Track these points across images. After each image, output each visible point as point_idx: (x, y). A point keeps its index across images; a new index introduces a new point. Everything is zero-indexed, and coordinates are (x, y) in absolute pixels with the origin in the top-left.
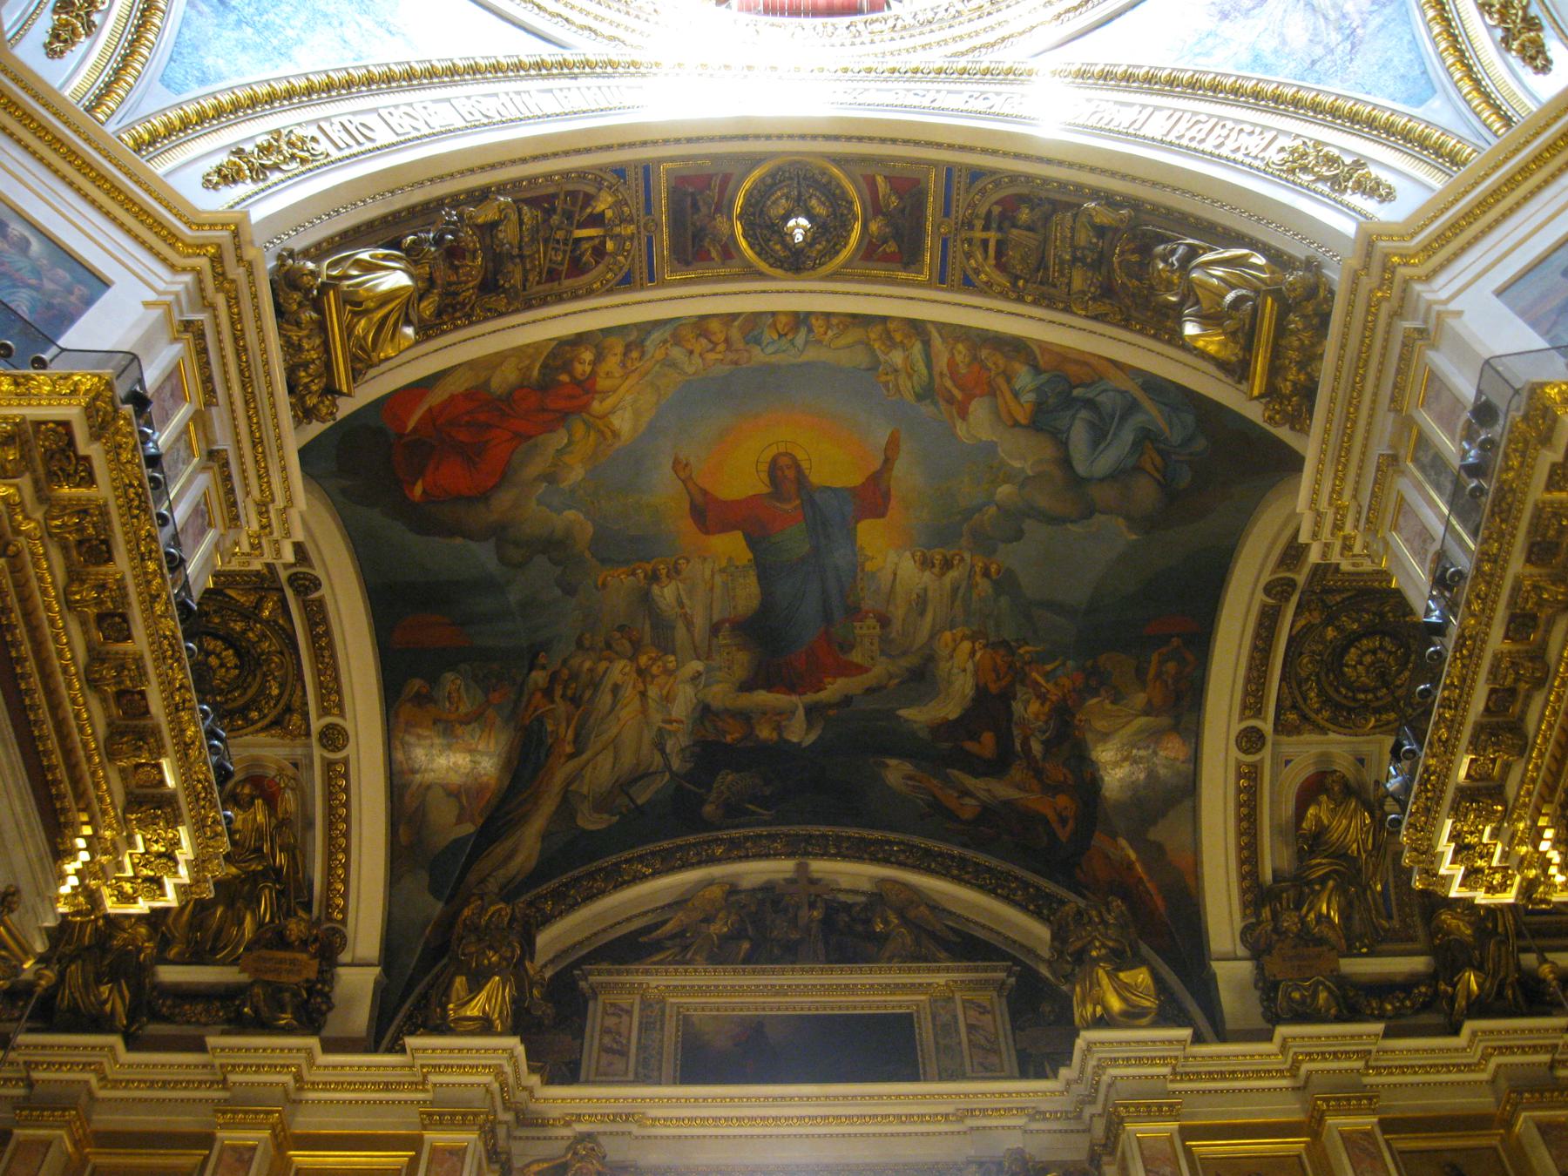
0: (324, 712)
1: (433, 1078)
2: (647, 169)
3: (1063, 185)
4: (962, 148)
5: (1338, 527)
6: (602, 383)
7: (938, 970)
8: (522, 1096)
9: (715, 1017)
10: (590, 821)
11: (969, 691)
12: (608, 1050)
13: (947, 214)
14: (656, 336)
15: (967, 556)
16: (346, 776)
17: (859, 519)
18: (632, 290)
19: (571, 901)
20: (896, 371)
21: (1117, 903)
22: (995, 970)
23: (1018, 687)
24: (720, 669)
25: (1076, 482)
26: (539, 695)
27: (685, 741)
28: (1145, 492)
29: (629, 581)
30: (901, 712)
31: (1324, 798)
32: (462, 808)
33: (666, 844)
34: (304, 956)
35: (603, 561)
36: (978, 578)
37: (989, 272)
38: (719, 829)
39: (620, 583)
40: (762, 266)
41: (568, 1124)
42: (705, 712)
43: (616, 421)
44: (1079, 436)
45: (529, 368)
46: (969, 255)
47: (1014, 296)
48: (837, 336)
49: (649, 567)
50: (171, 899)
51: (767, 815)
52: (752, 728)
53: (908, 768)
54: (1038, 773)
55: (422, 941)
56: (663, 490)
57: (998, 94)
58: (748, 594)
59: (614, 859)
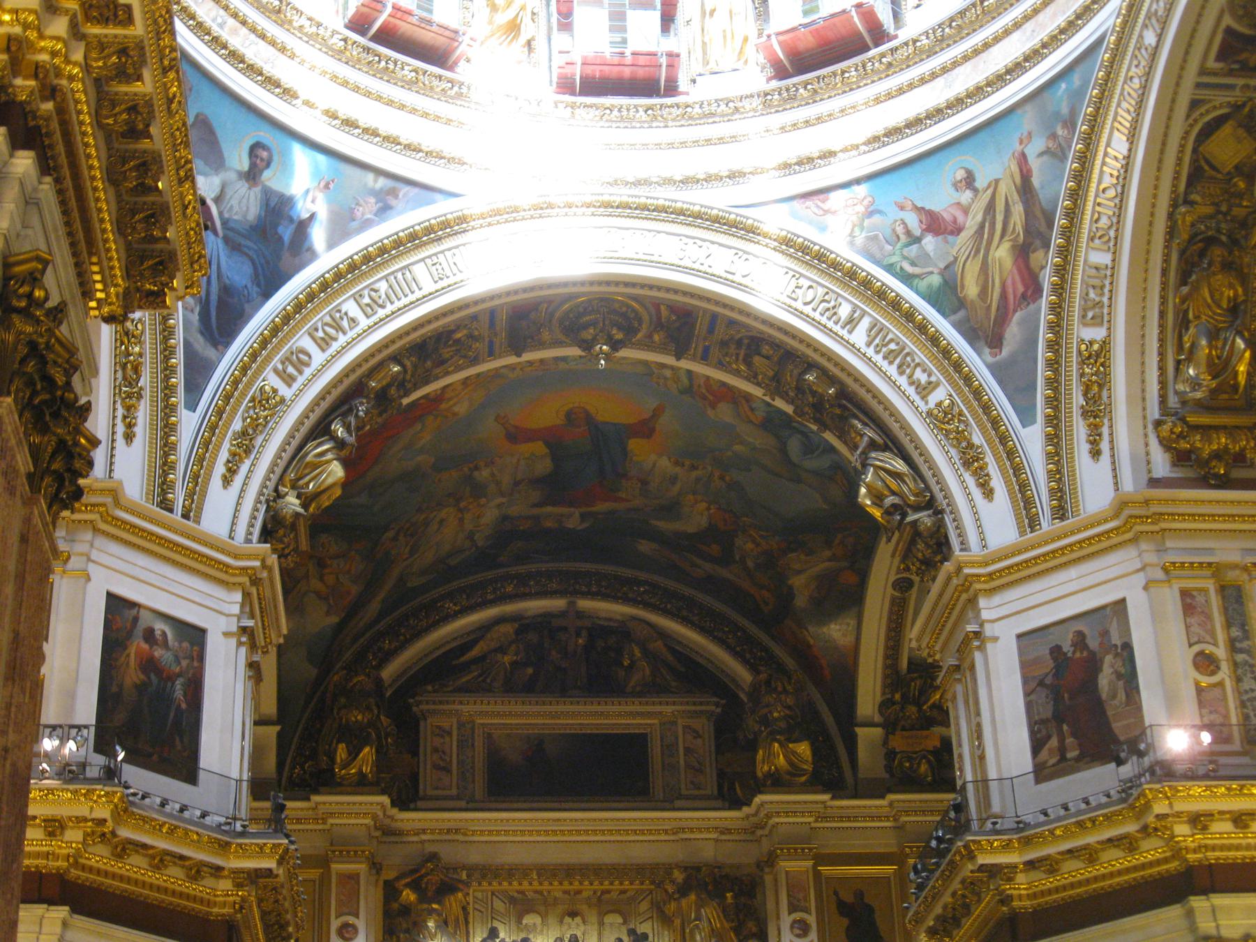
1: (331, 821)
6: (447, 396)
7: (667, 704)
8: (387, 821)
9: (508, 735)
11: (704, 522)
13: (711, 330)
20: (665, 378)
22: (708, 703)
33: (471, 579)
41: (417, 834)
42: (505, 518)
43: (456, 409)
44: (794, 446)
53: (654, 546)
58: (544, 466)
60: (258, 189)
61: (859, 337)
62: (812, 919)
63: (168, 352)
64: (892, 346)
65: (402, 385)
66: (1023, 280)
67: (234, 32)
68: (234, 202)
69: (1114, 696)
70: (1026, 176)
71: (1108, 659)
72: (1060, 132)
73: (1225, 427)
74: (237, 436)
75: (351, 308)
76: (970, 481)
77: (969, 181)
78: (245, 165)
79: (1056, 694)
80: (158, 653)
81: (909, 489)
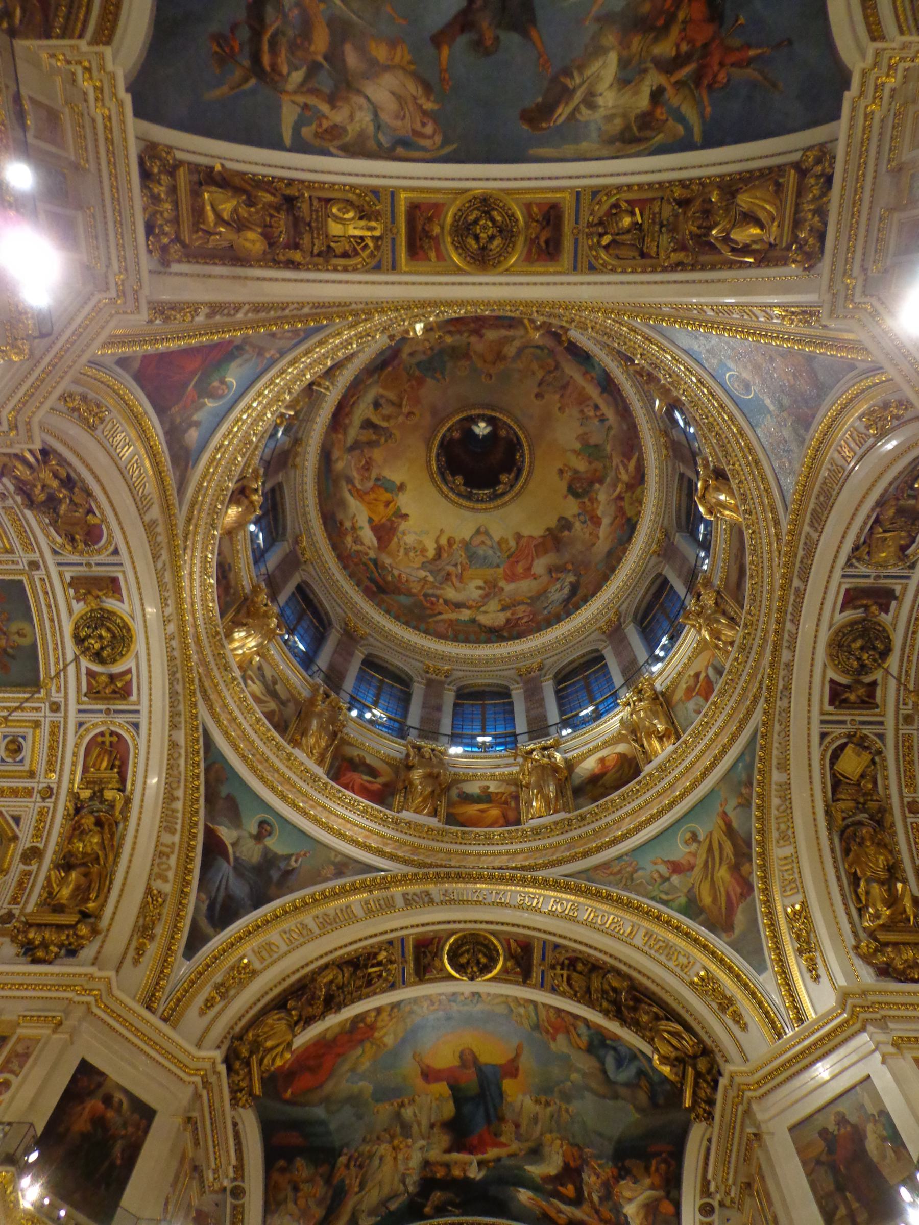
2: (403, 940)
3: (598, 959)
4: (550, 933)
6: (379, 1024)
13: (543, 959)
16: (242, 1213)
20: (520, 1015)
26: (342, 1168)
28: (642, 1097)
35: (377, 1101)
37: (564, 987)
39: (385, 1110)
40: (457, 976)
42: (426, 1164)
43: (386, 1040)
49: (400, 1101)
51: (457, 1211)
53: (530, 1194)
54: (597, 1212)
56: (409, 1068)
57: (568, 901)
58: (449, 1110)
60: (260, 846)
61: (639, 940)
63: (178, 916)
64: (661, 944)
65: (340, 988)
66: (738, 883)
67: (261, 762)
68: (244, 849)
69: (884, 1157)
70: (729, 825)
71: (870, 1127)
72: (744, 791)
73: (908, 944)
74: (217, 987)
75: (312, 925)
76: (730, 1023)
77: (694, 837)
78: (254, 830)
79: (833, 1168)
80: (110, 1114)
81: (688, 1043)
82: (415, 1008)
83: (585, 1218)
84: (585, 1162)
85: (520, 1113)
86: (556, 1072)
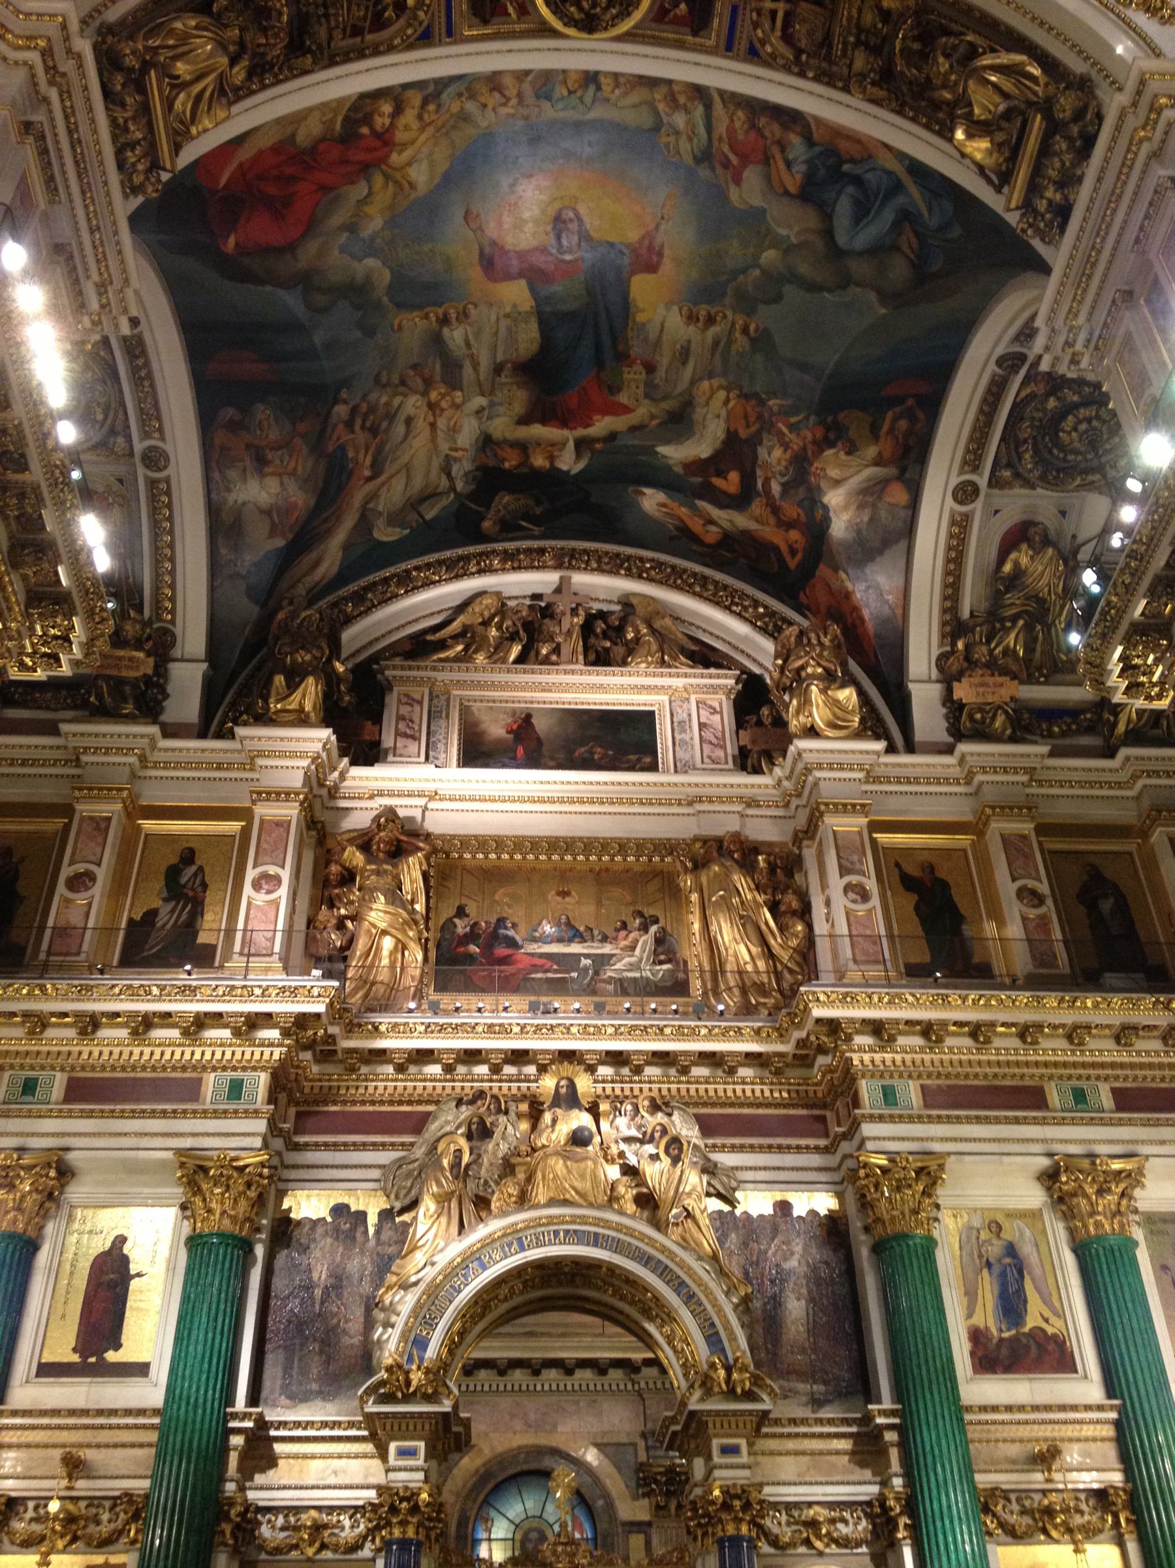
0: (146, 435)
1: (260, 762)
5: (1068, 344)
6: (400, 136)
10: (385, 534)
11: (721, 435)
12: (406, 736)
14: (452, 89)
15: (729, 313)
16: (168, 493)
17: (634, 273)
18: (430, 45)
19: (369, 604)
20: (677, 133)
21: (835, 629)
23: (765, 435)
24: (501, 404)
25: (836, 253)
26: (341, 426)
27: (467, 466)
28: (899, 270)
29: (422, 324)
30: (662, 450)
31: (1024, 547)
32: (273, 525)
33: (448, 554)
34: (141, 655)
35: (400, 306)
36: (737, 335)
37: (775, 44)
38: (497, 541)
39: (413, 326)
40: (557, 24)
42: (486, 442)
45: (332, 121)
46: (756, 25)
47: (796, 70)
48: (626, 94)
49: (440, 311)
50: (65, 670)
51: (537, 530)
52: (527, 457)
53: (661, 497)
54: (775, 510)
55: (242, 642)
58: (529, 338)
59: (403, 566)
62: (871, 885)
82: (470, 106)
83: (752, 526)
84: (766, 425)
85: (658, 343)
86: (735, 251)
